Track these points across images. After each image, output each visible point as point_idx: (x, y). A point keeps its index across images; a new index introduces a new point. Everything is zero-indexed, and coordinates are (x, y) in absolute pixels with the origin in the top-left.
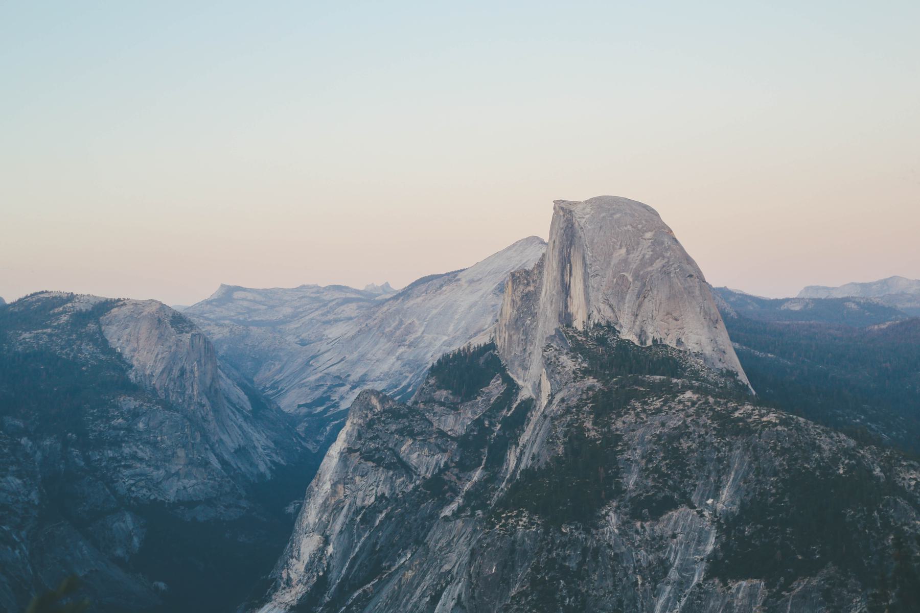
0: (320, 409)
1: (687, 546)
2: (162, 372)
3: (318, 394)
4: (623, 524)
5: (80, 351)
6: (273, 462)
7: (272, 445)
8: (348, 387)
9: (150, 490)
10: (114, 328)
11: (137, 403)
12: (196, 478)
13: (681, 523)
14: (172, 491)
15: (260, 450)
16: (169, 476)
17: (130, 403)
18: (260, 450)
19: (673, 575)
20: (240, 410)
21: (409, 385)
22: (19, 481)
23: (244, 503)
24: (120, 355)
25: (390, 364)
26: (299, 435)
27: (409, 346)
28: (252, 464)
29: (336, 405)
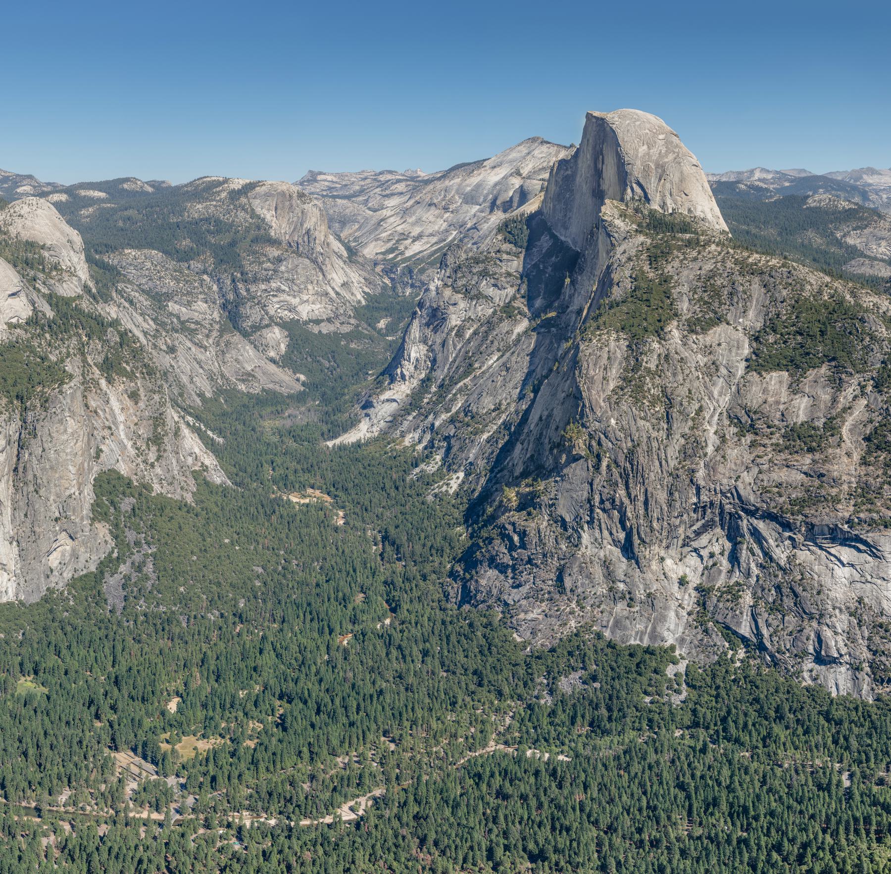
0: (391, 256)
1: (730, 350)
2: (294, 229)
3: (390, 245)
4: (684, 337)
5: (236, 216)
6: (364, 292)
7: (363, 281)
8: (410, 241)
9: (290, 311)
10: (257, 201)
11: (279, 252)
12: (321, 303)
13: (723, 335)
14: (305, 312)
15: (356, 284)
16: (303, 302)
17: (274, 252)
18: (356, 284)
19: (723, 371)
20: (340, 257)
21: (454, 239)
22: (205, 305)
23: (352, 321)
24: (263, 220)
25: (441, 225)
26: (379, 275)
27: (452, 212)
28: (352, 294)
29: (402, 253)
